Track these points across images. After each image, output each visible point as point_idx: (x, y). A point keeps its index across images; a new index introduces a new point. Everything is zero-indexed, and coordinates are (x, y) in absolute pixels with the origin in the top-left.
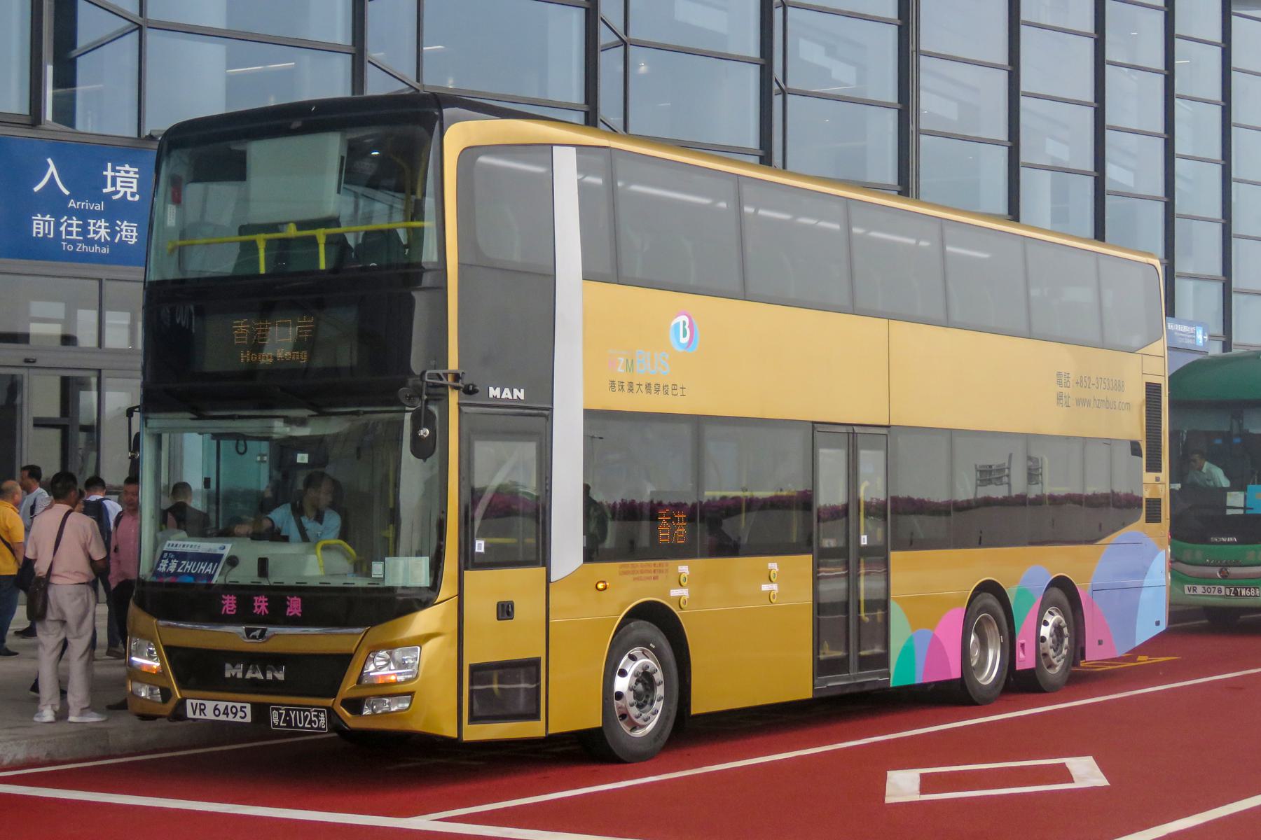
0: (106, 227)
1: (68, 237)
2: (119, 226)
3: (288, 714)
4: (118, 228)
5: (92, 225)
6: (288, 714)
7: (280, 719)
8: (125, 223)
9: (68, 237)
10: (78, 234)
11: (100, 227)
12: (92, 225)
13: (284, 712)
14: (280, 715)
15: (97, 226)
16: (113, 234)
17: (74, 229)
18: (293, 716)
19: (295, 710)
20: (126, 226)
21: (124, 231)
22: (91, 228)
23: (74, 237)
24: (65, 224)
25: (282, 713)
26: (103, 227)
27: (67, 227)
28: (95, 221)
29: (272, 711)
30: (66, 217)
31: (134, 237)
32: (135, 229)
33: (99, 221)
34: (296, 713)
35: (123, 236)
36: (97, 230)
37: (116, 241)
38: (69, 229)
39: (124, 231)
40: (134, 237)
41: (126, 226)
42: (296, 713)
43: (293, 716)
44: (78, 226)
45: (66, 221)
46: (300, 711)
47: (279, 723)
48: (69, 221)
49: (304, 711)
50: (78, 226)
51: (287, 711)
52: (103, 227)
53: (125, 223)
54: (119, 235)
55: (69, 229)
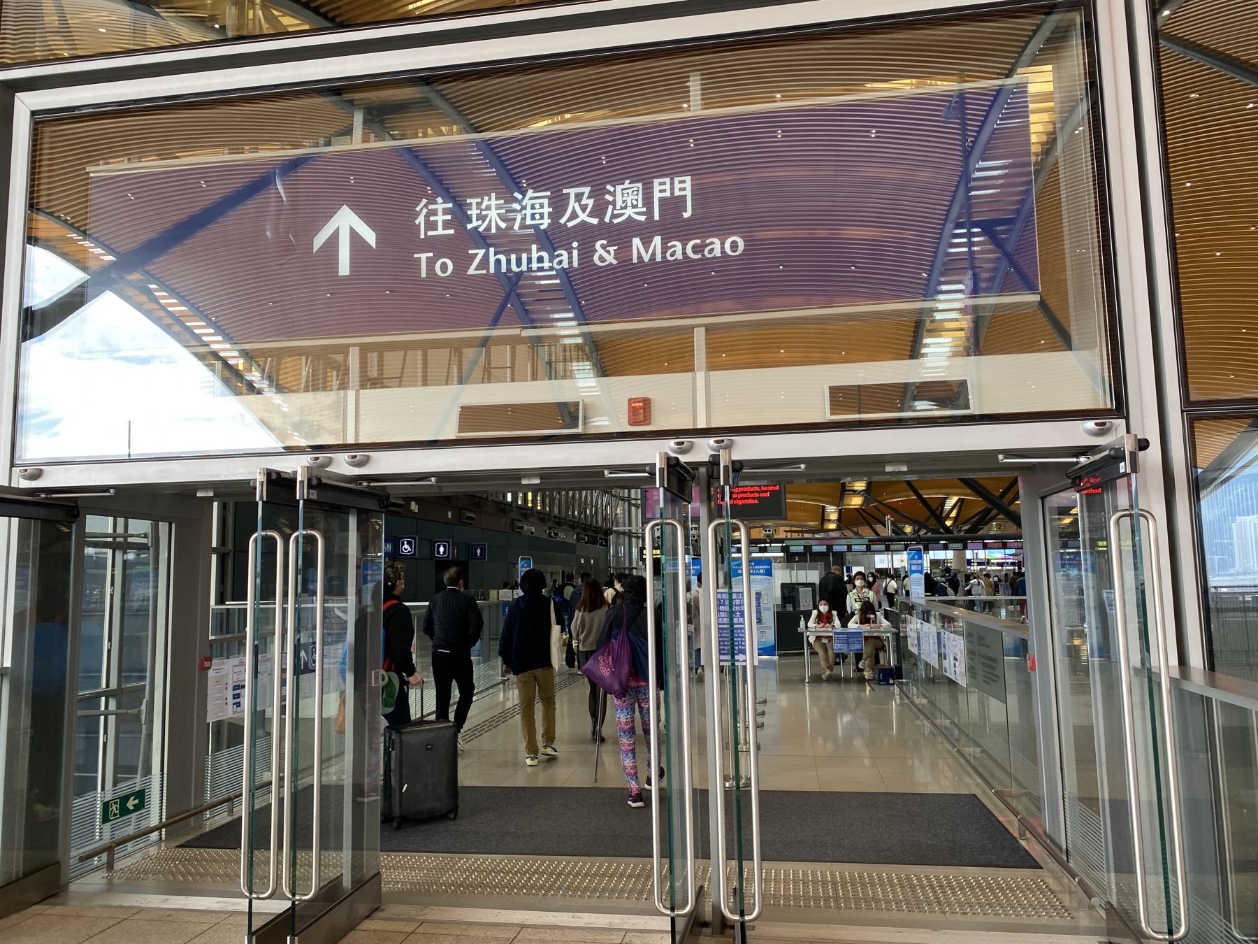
0: (498, 207)
1: (430, 233)
2: (519, 202)
5: (474, 206)
8: (530, 193)
9: (430, 233)
10: (446, 225)
12: (474, 206)
15: (483, 207)
20: (531, 198)
21: (529, 207)
22: (473, 212)
23: (440, 231)
24: (425, 211)
27: (427, 217)
28: (479, 200)
30: (424, 201)
31: (546, 216)
32: (546, 202)
33: (486, 198)
35: (528, 217)
38: (432, 218)
39: (529, 207)
40: (546, 216)
41: (531, 198)
44: (445, 212)
45: (426, 206)
48: (431, 207)
50: (445, 212)
53: (530, 193)
55: (432, 218)
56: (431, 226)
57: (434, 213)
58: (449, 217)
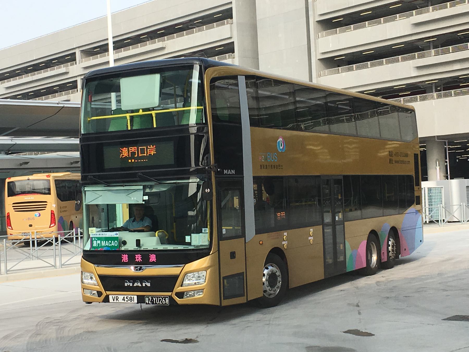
3: (152, 299)
6: (152, 299)
7: (149, 301)
13: (151, 298)
14: (149, 299)
18: (154, 299)
19: (156, 297)
25: (150, 299)
29: (146, 297)
34: (156, 299)
42: (156, 299)
43: (154, 299)
46: (157, 298)
47: (149, 302)
49: (159, 297)
51: (152, 298)
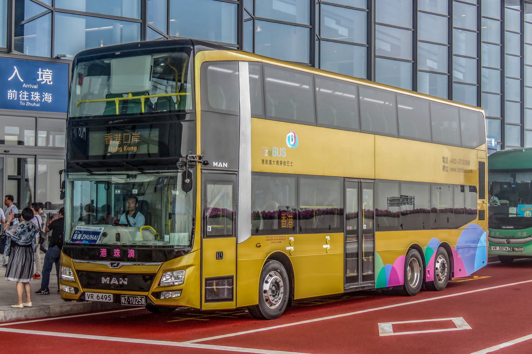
0: (38, 95)
1: (22, 99)
2: (44, 95)
4: (43, 96)
8: (47, 94)
9: (22, 99)
10: (27, 98)
11: (36, 95)
16: (41, 98)
17: (25, 96)
20: (47, 95)
21: (46, 97)
22: (32, 96)
23: (25, 99)
24: (22, 94)
26: (37, 95)
27: (22, 95)
28: (34, 93)
30: (22, 91)
31: (50, 100)
32: (50, 96)
33: (36, 93)
35: (46, 99)
36: (35, 96)
37: (43, 101)
38: (23, 96)
40: (50, 100)
41: (47, 95)
44: (27, 95)
45: (22, 93)
48: (23, 93)
50: (27, 95)
52: (37, 95)
53: (47, 94)
54: (44, 98)
55: (23, 96)
56: (23, 98)
57: (24, 94)
58: (28, 96)
